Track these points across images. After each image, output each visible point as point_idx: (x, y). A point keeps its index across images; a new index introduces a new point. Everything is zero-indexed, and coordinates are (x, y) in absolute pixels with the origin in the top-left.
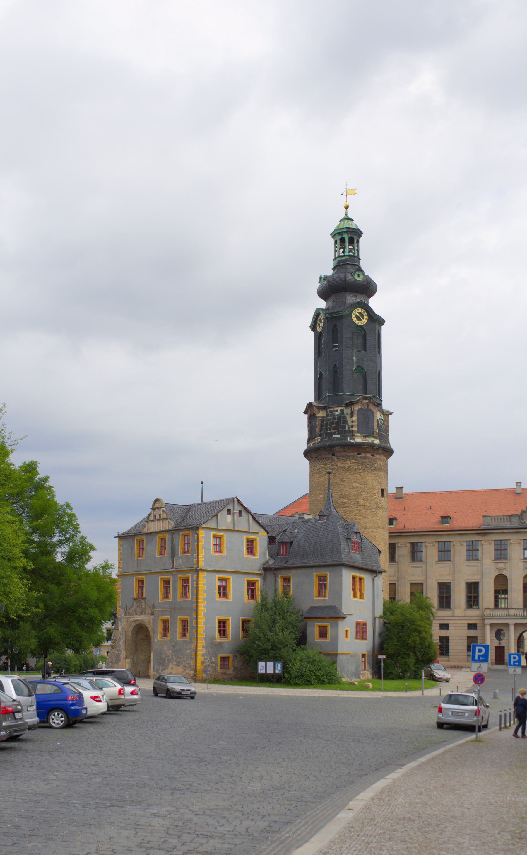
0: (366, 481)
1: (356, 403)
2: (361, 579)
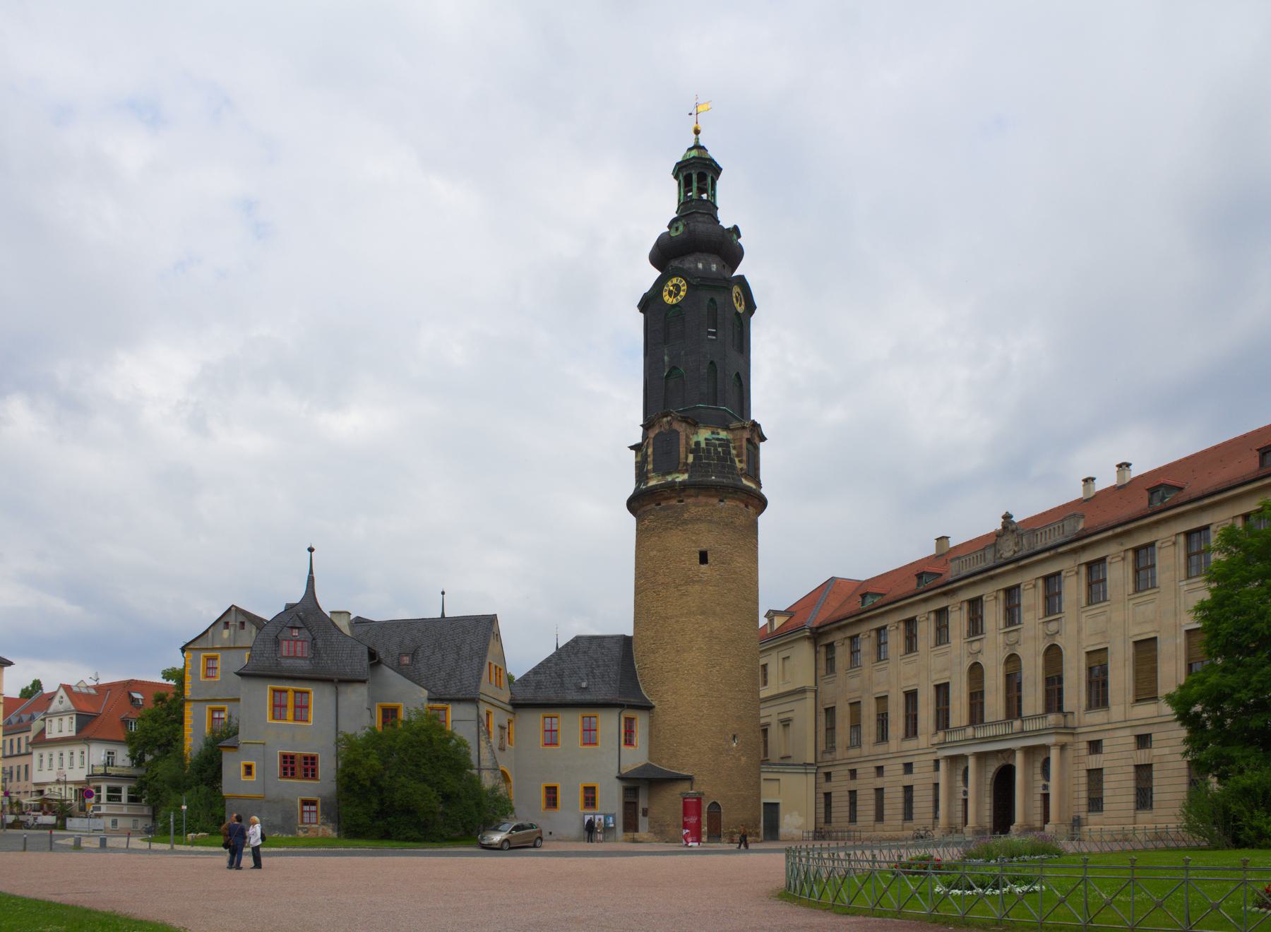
0: (668, 545)
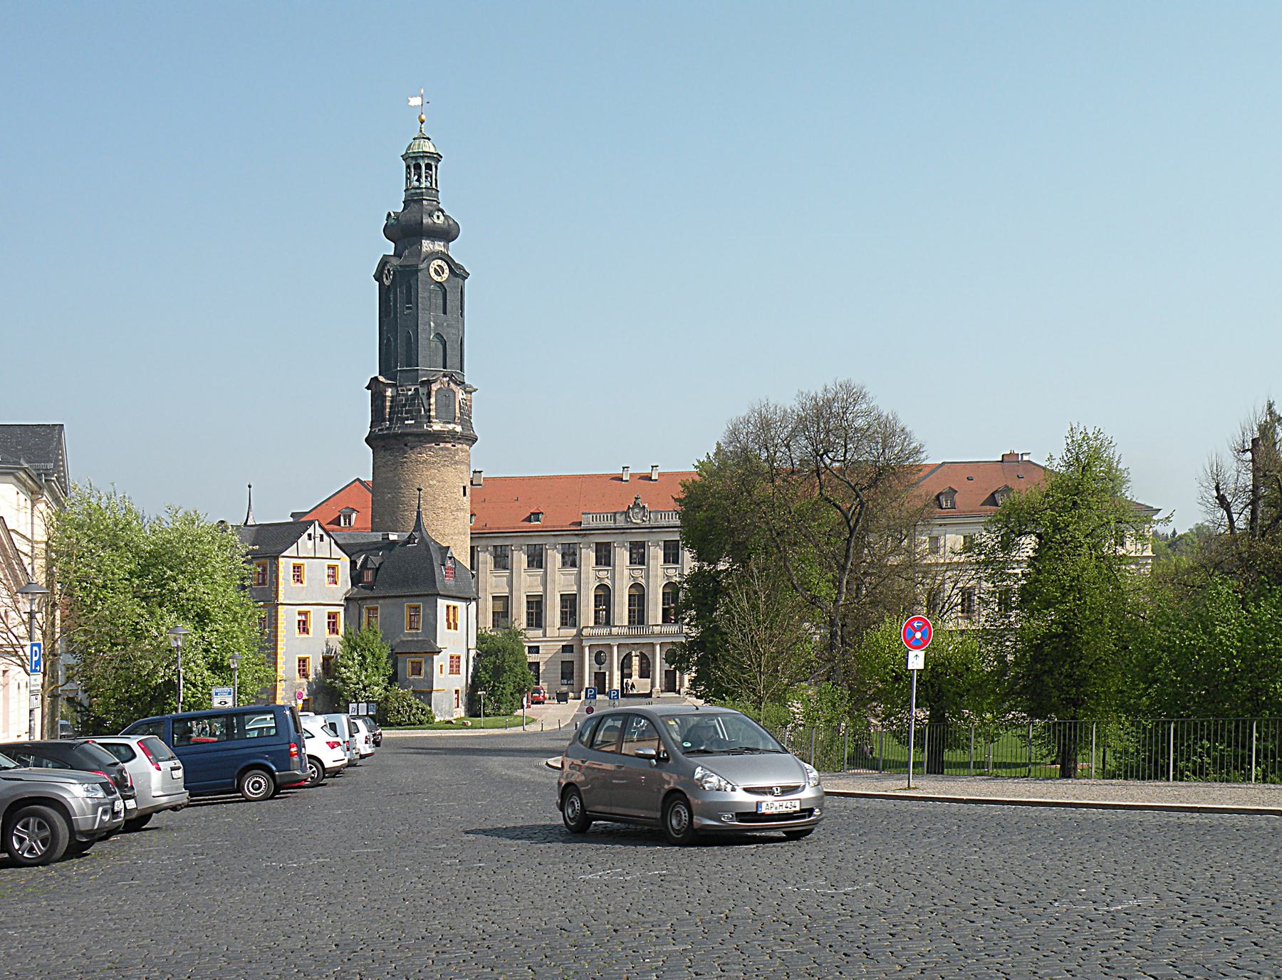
1: (435, 381)
2: (454, 608)
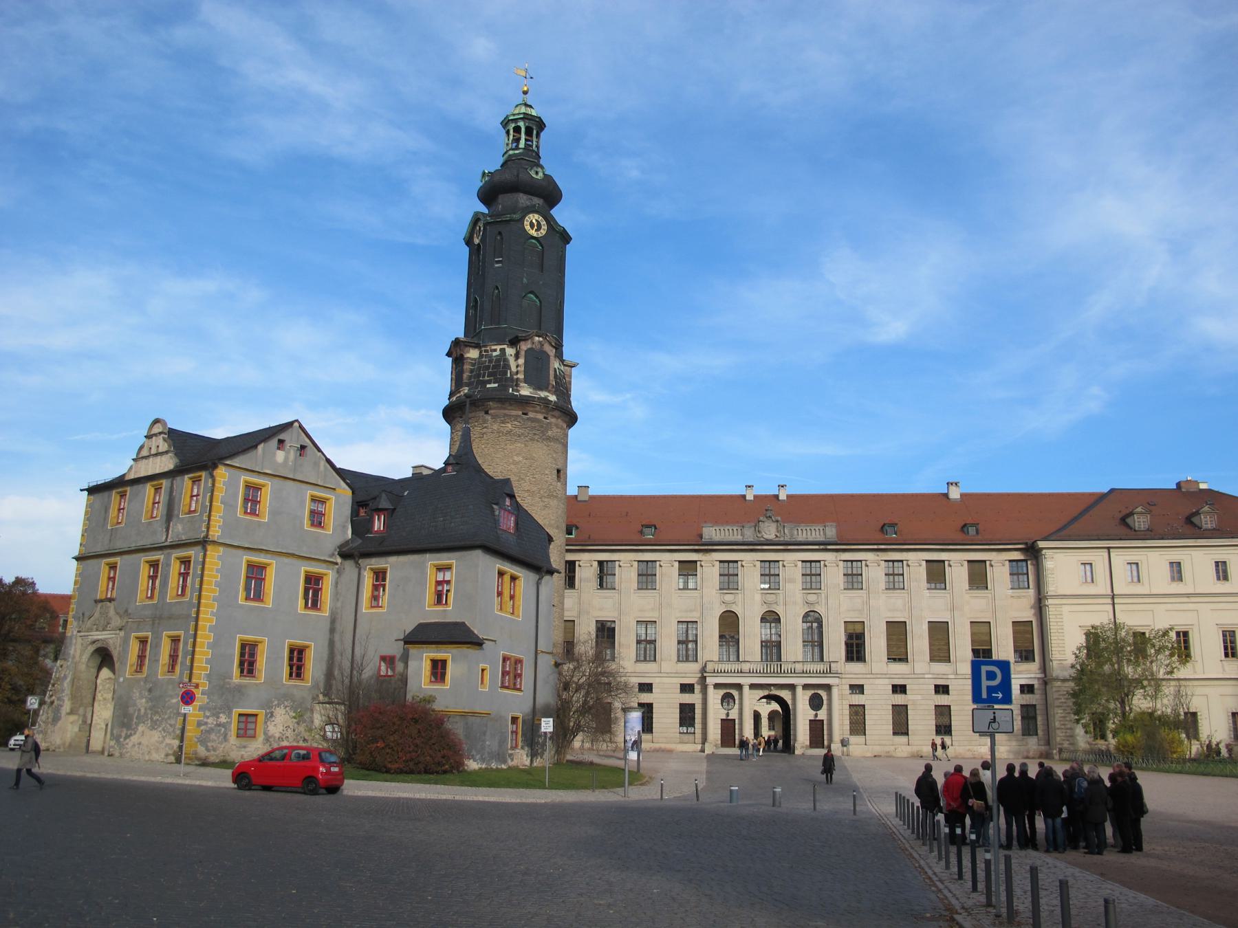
1: (526, 340)
